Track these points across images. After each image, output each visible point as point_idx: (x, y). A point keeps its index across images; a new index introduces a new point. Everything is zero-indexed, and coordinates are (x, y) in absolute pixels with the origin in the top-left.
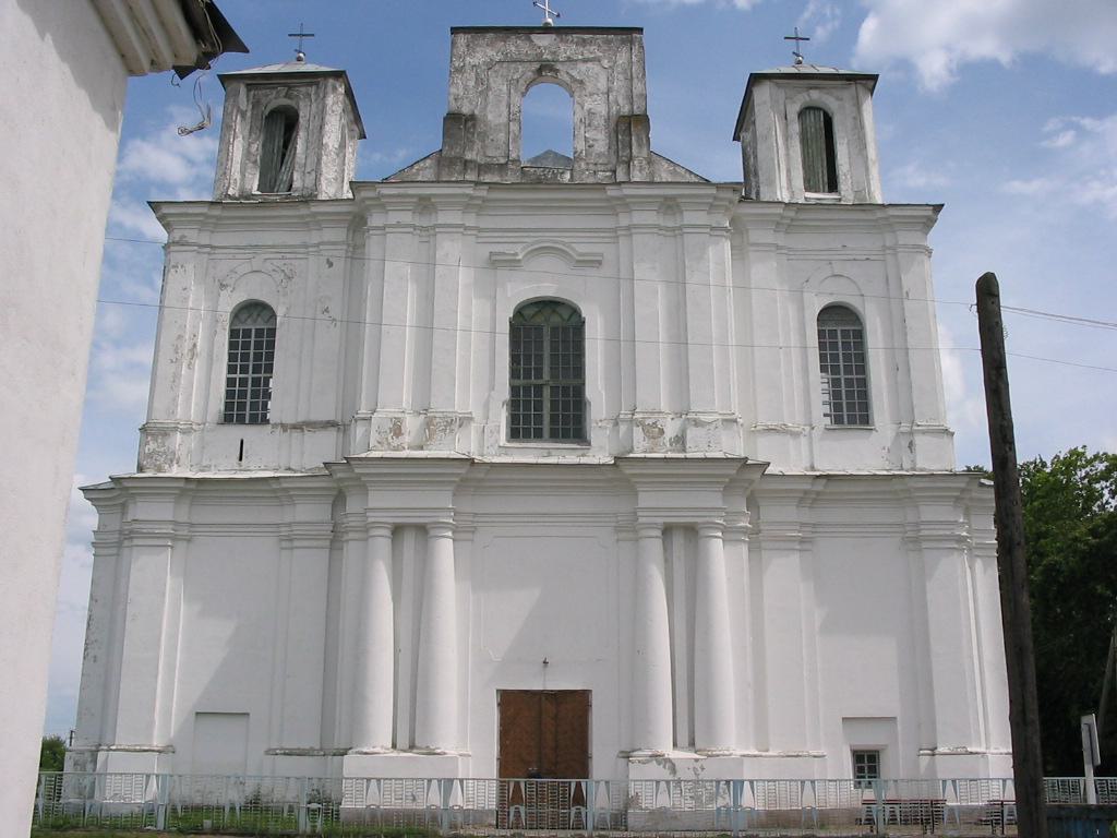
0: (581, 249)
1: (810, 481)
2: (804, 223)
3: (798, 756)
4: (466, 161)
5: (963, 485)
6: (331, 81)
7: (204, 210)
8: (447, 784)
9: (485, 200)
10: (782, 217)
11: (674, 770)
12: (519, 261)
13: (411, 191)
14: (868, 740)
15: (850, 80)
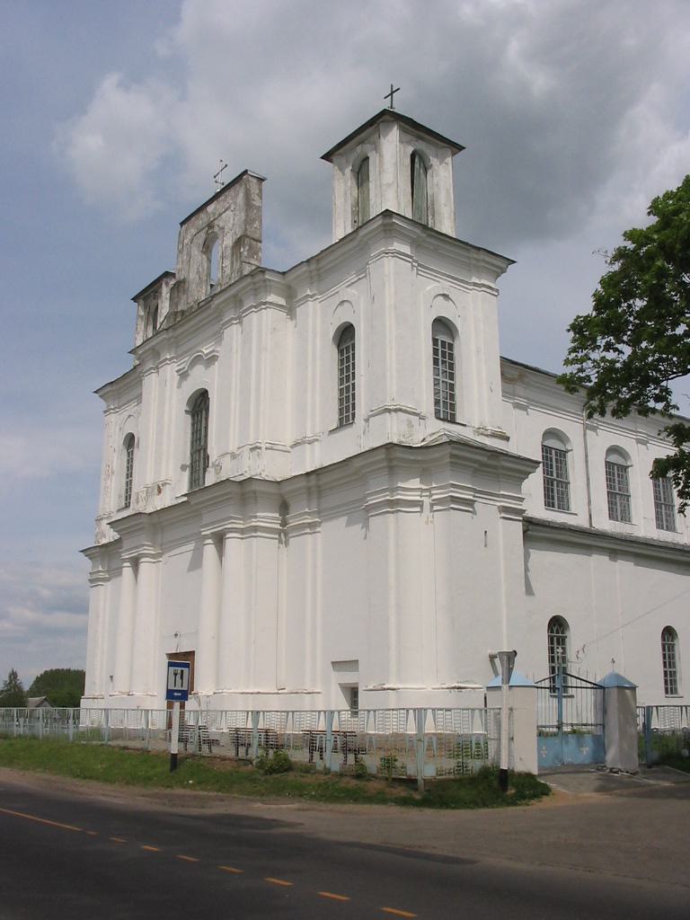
0: (206, 352)
1: (303, 478)
2: (326, 268)
3: (297, 693)
4: (183, 312)
5: (383, 456)
6: (165, 279)
7: (109, 388)
8: (420, 713)
9: (176, 337)
10: (311, 272)
11: (200, 705)
12: (187, 371)
13: (147, 348)
14: (349, 678)
15: (371, 125)
